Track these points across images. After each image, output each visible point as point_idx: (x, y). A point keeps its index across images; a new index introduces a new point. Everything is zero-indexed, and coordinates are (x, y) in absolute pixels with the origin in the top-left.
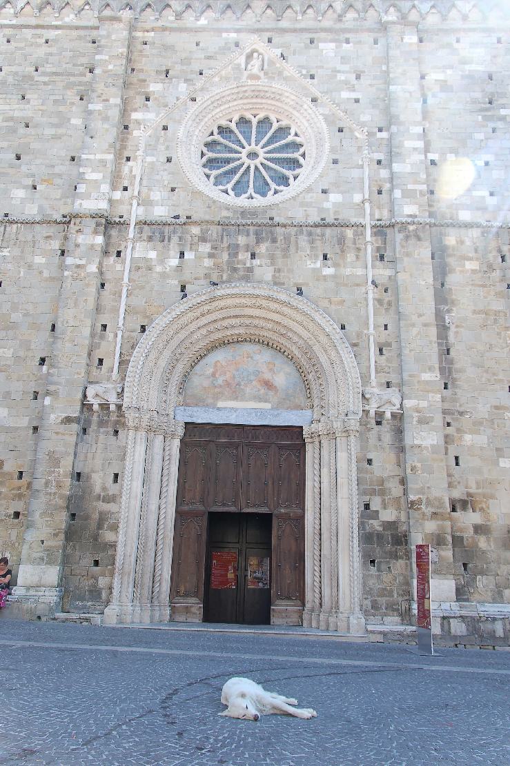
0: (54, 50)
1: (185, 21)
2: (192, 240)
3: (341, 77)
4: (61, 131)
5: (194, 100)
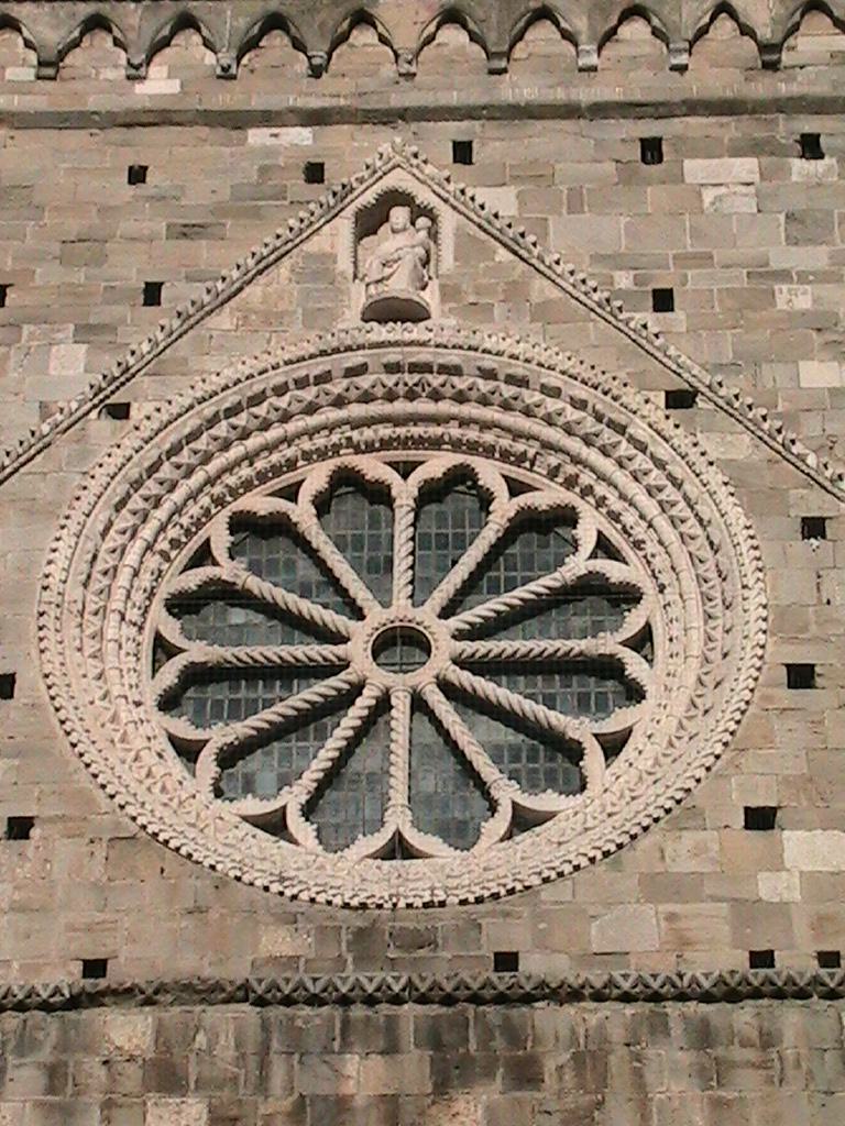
1: (78, 86)
3: (801, 299)
5: (120, 412)
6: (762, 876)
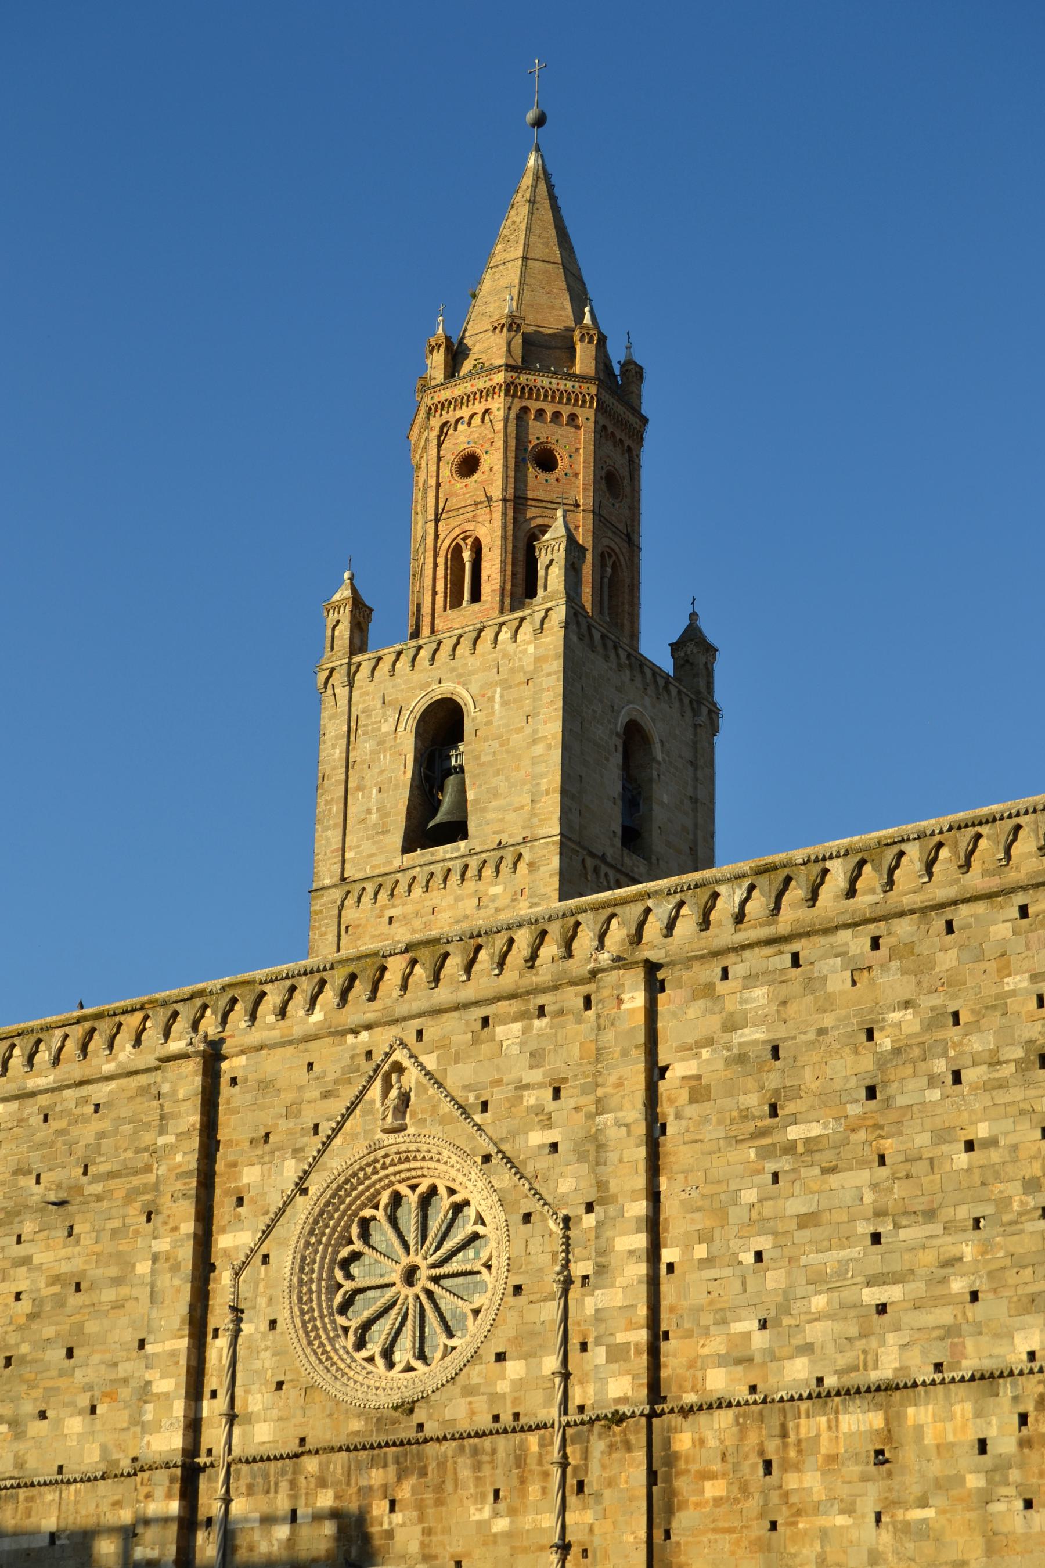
0: (106, 1125)
2: (308, 1483)
3: (530, 1098)
4: (124, 1291)
5: (304, 1191)
6: (499, 1382)
